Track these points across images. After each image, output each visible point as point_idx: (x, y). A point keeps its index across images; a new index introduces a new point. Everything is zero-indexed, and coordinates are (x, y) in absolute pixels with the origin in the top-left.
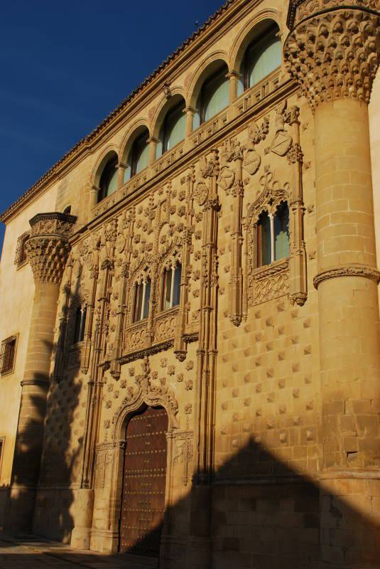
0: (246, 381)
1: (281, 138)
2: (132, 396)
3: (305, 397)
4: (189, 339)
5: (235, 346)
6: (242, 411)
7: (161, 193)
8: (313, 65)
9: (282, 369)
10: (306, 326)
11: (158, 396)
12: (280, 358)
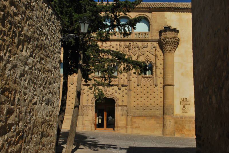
0: (141, 97)
1: (152, 50)
3: (157, 102)
4: (123, 86)
5: (138, 90)
6: (140, 103)
7: (106, 44)
8: (170, 45)
9: (151, 97)
10: (157, 90)
12: (151, 95)
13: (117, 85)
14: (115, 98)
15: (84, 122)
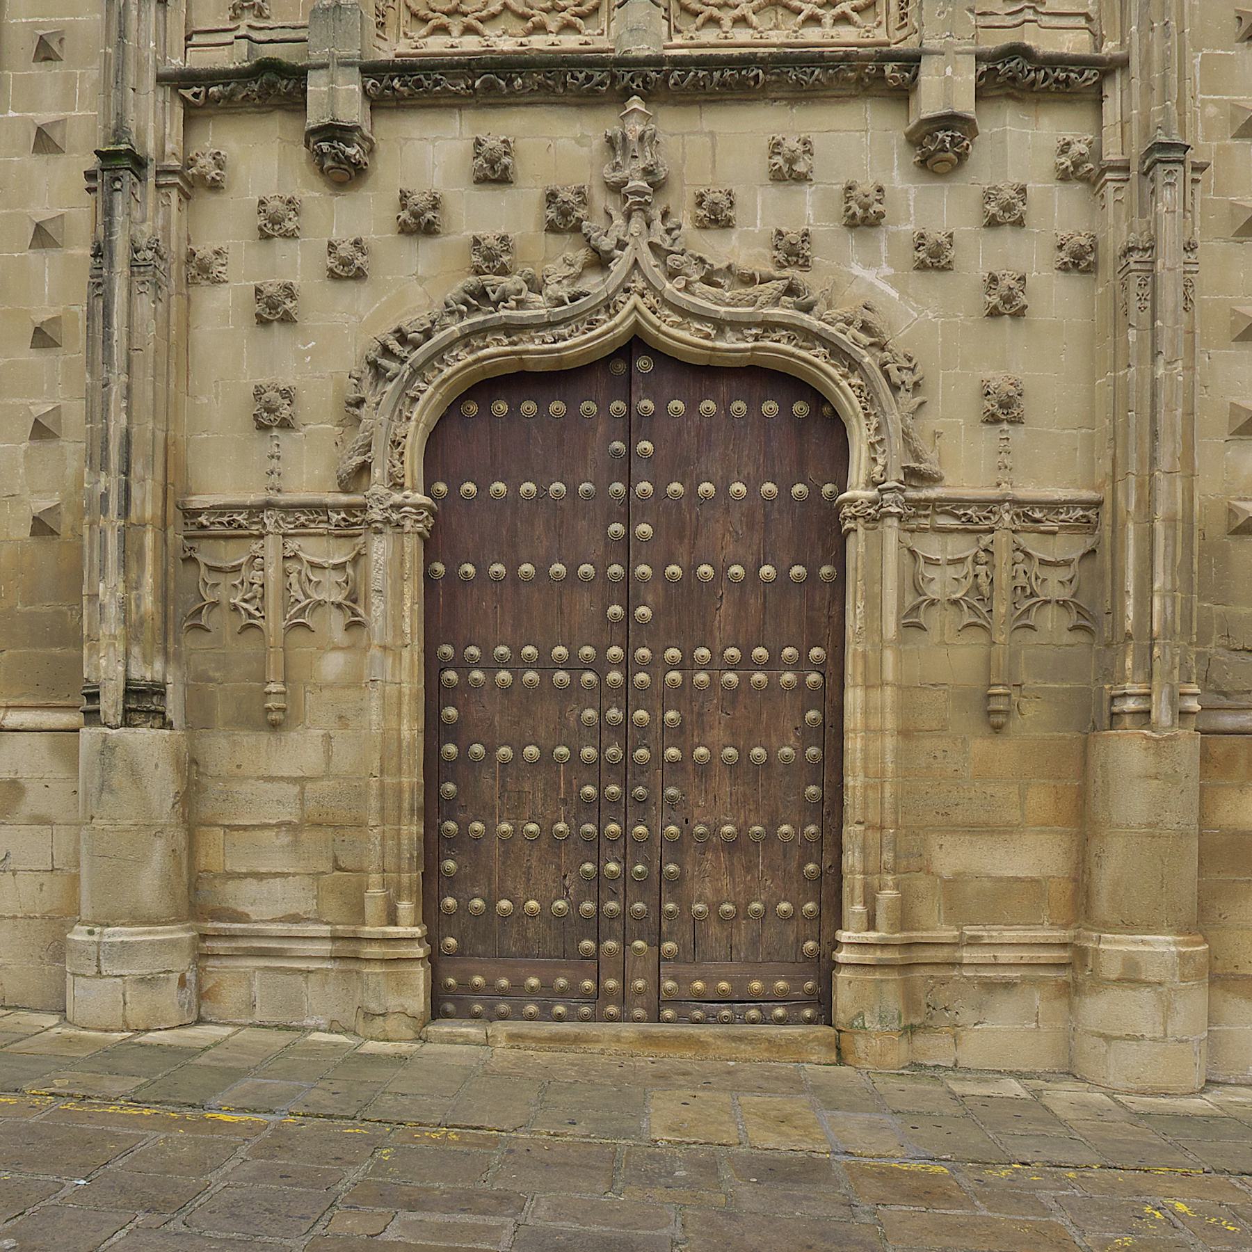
2: (536, 286)
11: (776, 313)
13: (885, 77)
14: (848, 337)
15: (218, 852)
